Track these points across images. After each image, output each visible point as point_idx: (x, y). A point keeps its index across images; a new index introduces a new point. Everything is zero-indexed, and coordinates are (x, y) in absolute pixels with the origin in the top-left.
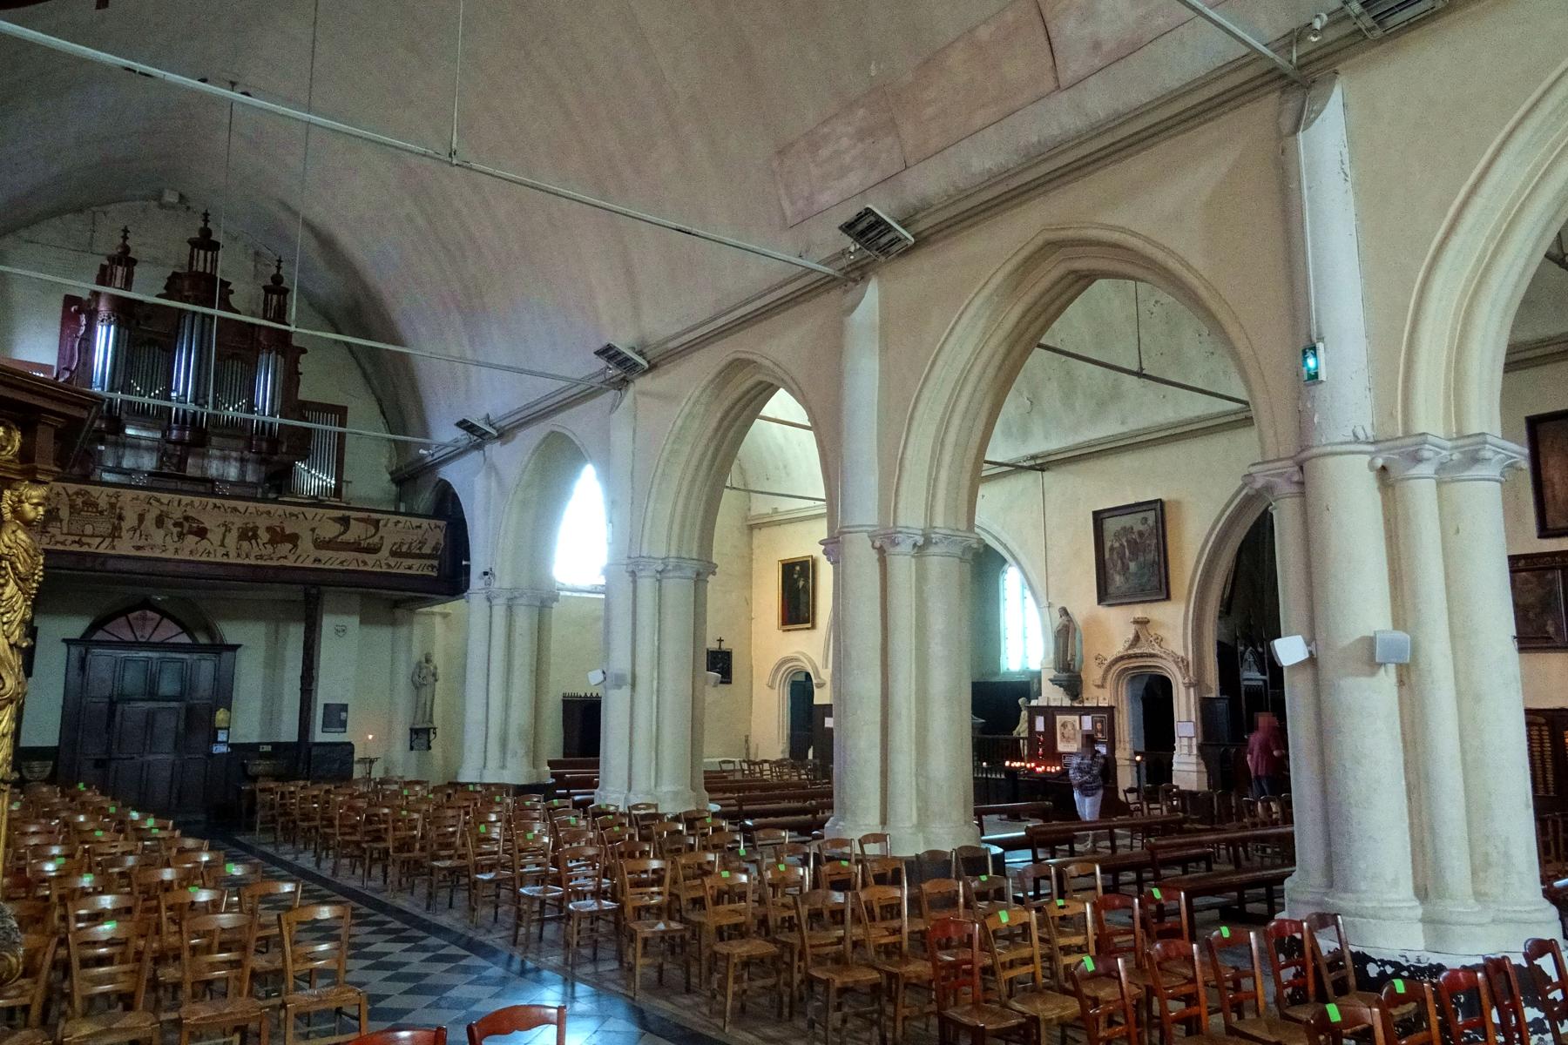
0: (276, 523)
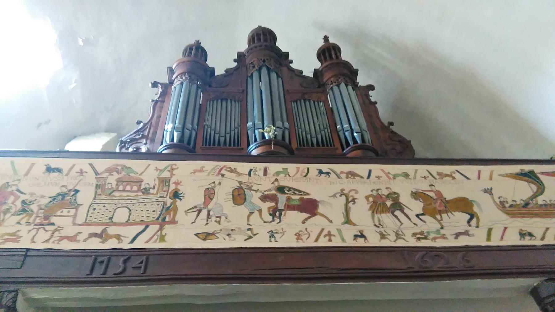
0: (423, 186)
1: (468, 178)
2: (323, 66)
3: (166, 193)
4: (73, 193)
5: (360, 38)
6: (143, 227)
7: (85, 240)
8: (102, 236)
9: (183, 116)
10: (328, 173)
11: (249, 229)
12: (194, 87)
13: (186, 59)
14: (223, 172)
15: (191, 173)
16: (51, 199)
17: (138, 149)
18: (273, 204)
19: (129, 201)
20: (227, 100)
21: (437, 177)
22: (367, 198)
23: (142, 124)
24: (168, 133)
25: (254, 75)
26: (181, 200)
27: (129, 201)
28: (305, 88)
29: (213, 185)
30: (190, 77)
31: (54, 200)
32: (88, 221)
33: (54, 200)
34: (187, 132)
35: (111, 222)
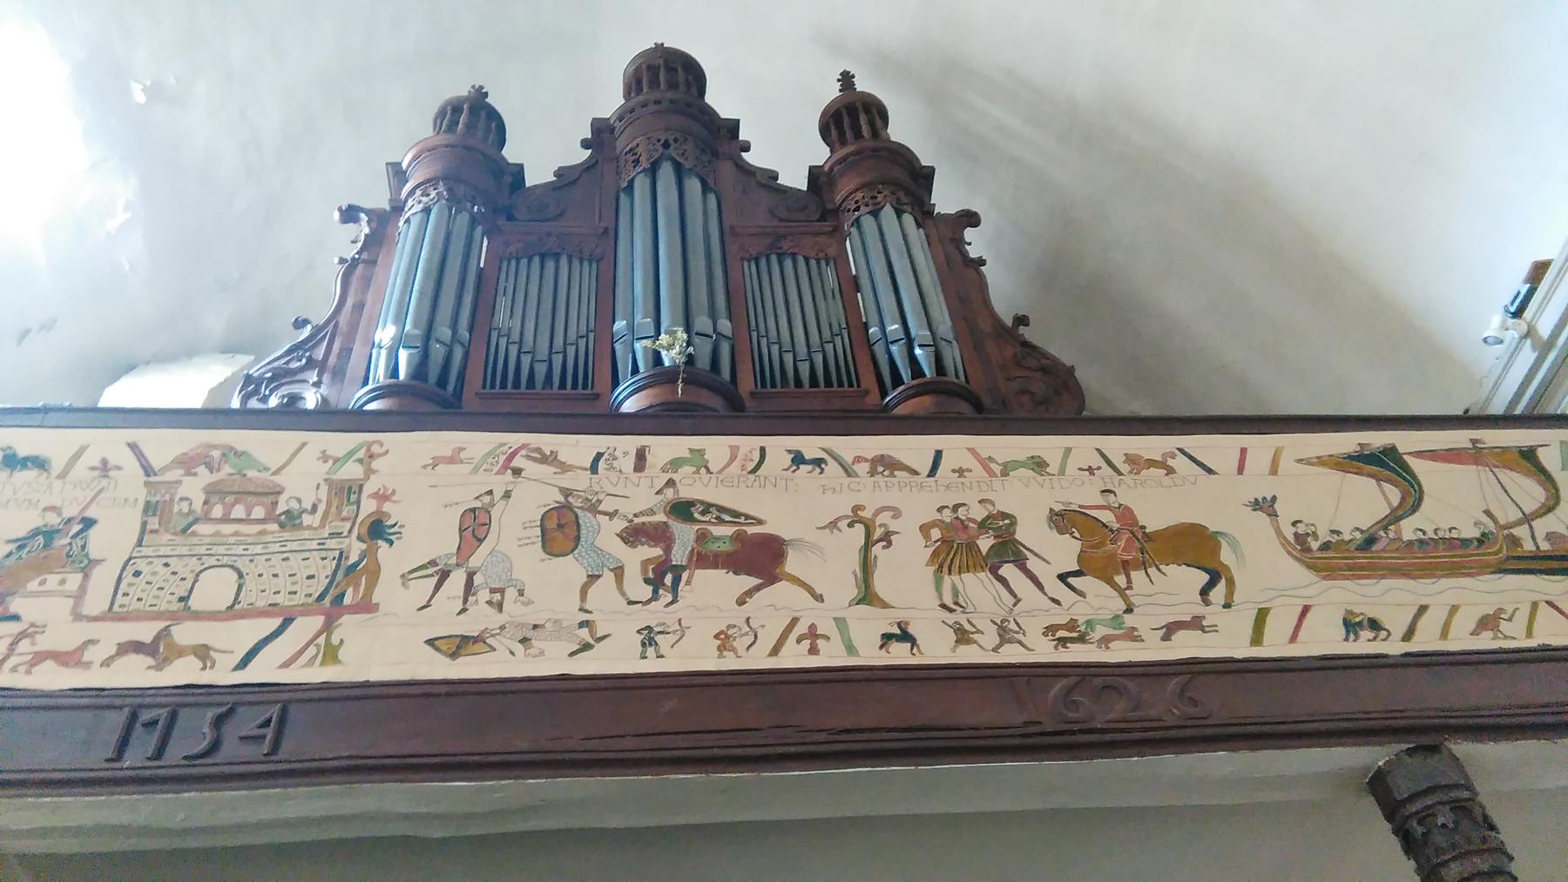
0: (1084, 494)
1: (1210, 471)
2: (838, 155)
3: (348, 525)
4: (76, 528)
5: (943, 78)
6: (276, 623)
7: (106, 663)
8: (156, 650)
9: (427, 304)
10: (818, 462)
11: (582, 625)
12: (464, 219)
13: (443, 139)
14: (518, 462)
15: (425, 467)
16: (12, 547)
17: (294, 399)
18: (657, 552)
19: (239, 550)
20: (557, 257)
21: (1125, 468)
22: (925, 529)
23: (309, 327)
24: (384, 352)
25: (637, 184)
26: (391, 543)
27: (239, 550)
28: (781, 220)
29: (487, 499)
30: (449, 190)
31: (20, 548)
32: (116, 608)
33: (20, 548)
34: (437, 351)
35: (185, 610)
